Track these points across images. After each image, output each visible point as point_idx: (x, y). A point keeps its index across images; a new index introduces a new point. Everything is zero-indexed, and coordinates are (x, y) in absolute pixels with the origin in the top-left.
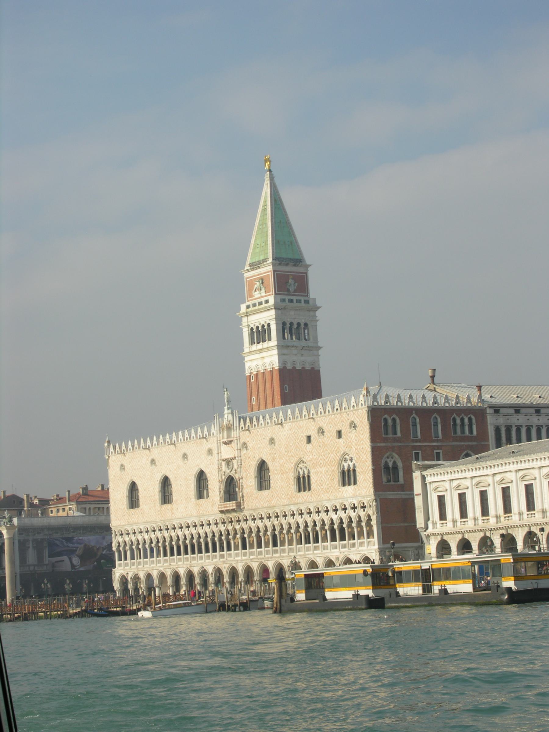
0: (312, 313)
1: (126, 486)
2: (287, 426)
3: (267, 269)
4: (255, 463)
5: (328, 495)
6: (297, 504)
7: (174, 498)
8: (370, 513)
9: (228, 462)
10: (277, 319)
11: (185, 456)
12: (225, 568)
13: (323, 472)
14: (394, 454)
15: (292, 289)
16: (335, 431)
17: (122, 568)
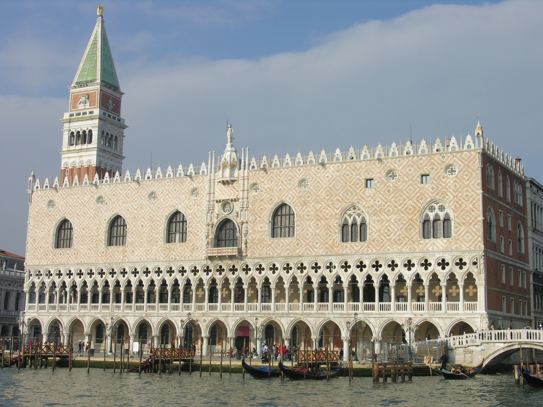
0: (121, 130)
1: (54, 223)
2: (331, 168)
3: (95, 88)
5: (399, 248)
6: (343, 255)
7: (129, 239)
8: (474, 270)
9: (225, 204)
10: (100, 127)
12: (205, 321)
13: (392, 221)
14: (492, 209)
15: (111, 107)
16: (419, 174)
17: (36, 311)
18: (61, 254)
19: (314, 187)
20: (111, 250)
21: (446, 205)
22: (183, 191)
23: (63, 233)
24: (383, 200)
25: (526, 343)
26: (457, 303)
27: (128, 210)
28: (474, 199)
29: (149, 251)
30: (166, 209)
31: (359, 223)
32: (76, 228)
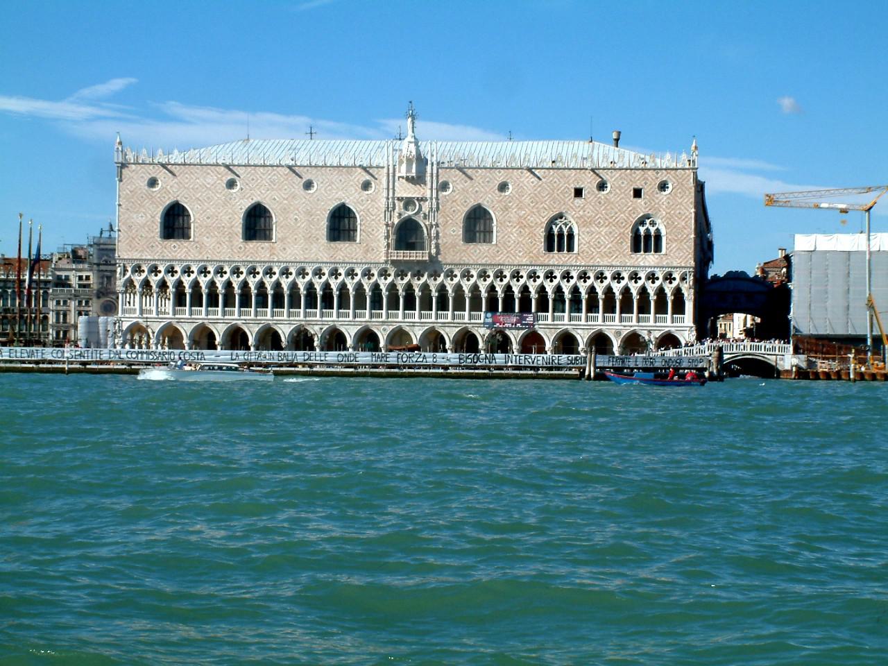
4: (466, 209)
9: (408, 202)
11: (308, 185)
12: (384, 330)
18: (175, 247)
19: (517, 192)
20: (251, 246)
21: (658, 221)
22: (351, 183)
23: (175, 222)
24: (593, 212)
25: (749, 354)
26: (665, 316)
27: (275, 199)
28: (686, 217)
29: (306, 249)
30: (329, 202)
31: (566, 233)
32: (197, 216)
